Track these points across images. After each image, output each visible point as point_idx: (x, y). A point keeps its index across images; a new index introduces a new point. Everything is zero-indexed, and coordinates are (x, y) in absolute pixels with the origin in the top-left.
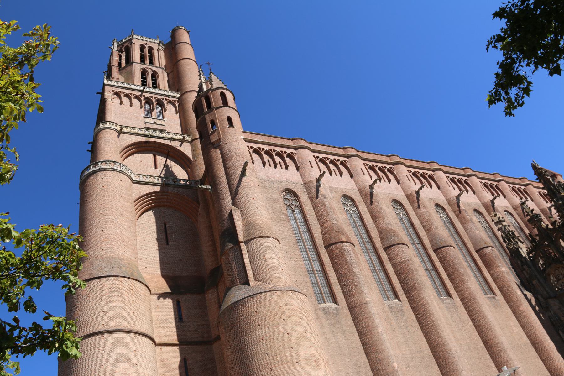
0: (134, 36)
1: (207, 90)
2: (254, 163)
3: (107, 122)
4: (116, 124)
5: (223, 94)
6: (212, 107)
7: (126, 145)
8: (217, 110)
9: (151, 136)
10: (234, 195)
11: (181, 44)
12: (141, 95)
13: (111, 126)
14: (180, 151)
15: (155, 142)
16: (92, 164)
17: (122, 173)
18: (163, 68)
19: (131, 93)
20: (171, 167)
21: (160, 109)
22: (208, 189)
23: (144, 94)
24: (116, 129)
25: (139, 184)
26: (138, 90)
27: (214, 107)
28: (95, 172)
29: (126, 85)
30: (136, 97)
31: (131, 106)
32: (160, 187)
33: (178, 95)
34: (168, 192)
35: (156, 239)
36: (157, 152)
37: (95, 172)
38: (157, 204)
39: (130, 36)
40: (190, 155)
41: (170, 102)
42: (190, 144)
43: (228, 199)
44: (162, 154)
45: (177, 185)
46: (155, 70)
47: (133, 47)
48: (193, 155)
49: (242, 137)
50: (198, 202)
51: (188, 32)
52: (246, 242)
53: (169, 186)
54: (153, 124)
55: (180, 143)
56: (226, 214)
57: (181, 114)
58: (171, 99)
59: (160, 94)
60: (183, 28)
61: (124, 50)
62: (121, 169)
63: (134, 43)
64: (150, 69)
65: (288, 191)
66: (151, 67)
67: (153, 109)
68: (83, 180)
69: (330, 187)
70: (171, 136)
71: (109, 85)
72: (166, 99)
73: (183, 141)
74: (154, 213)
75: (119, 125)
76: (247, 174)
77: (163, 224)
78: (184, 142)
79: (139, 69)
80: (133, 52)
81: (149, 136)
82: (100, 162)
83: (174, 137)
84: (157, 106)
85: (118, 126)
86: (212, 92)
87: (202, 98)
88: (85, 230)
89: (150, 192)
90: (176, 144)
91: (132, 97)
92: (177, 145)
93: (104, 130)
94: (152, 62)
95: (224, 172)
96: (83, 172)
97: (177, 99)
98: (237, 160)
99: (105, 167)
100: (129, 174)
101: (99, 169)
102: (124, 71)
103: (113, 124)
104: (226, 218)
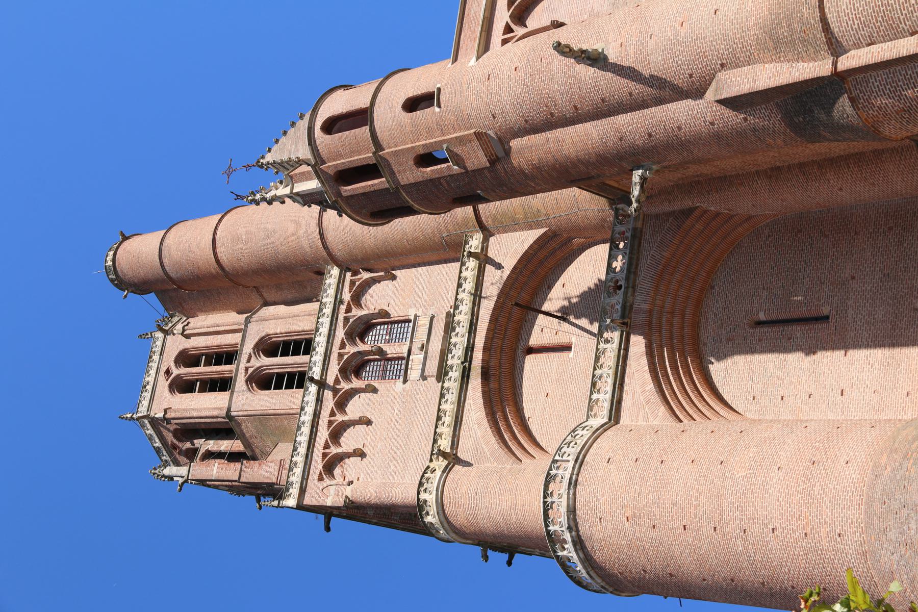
0: (143, 411)
1: (319, 178)
2: (561, 20)
3: (418, 499)
4: (425, 472)
5: (331, 126)
6: (374, 162)
7: (493, 440)
8: (384, 144)
9: (465, 361)
10: (667, 92)
11: (166, 262)
12: (335, 391)
13: (432, 486)
14: (515, 268)
15: (486, 349)
16: (555, 552)
17: (584, 456)
18: (247, 321)
19: (326, 423)
20: (569, 299)
21: (381, 330)
22: (643, 179)
23: (330, 380)
24: (444, 472)
25: (619, 402)
26: (319, 400)
27: (374, 153)
28: (579, 543)
29: (303, 439)
30: (341, 405)
31: (368, 422)
32: (632, 336)
33: (335, 271)
34: (650, 312)
35: (807, 354)
36: (518, 341)
37: (579, 543)
38: (687, 348)
39: (143, 426)
40: (529, 237)
41: (357, 299)
42: (492, 235)
44: (524, 326)
45: (627, 279)
46: (252, 346)
47: (178, 415)
48: (531, 228)
49: (473, 62)
50: (687, 213)
51: (125, 238)
52: (836, 48)
53: (631, 306)
54: (426, 353)
55: (489, 268)
56: (733, 118)
57: (397, 263)
58: (347, 296)
59: (330, 330)
60: (111, 253)
61: (188, 445)
62: (572, 458)
63: (165, 411)
64: (249, 361)
66: (244, 358)
67: (380, 352)
68: (603, 584)
70: (466, 297)
71: (303, 491)
72: (348, 310)
73: (482, 257)
74: (719, 358)
75: (431, 460)
76: (599, 47)
77: (758, 330)
78: (486, 255)
79: (249, 394)
80: (195, 414)
81: (464, 367)
82: (547, 526)
83: (469, 286)
84: (370, 338)
85: (432, 465)
86: (324, 162)
87: (344, 194)
88: (771, 589)
89: (647, 368)
90: (494, 281)
91: (340, 418)
92: (497, 277)
93: (446, 509)
94: (228, 356)
95: (588, 125)
96: (579, 582)
97: (349, 274)
98: (551, 81)
99: (563, 509)
100: (587, 434)
101: (570, 528)
102: (256, 442)
103: (428, 479)
104: (745, 119)
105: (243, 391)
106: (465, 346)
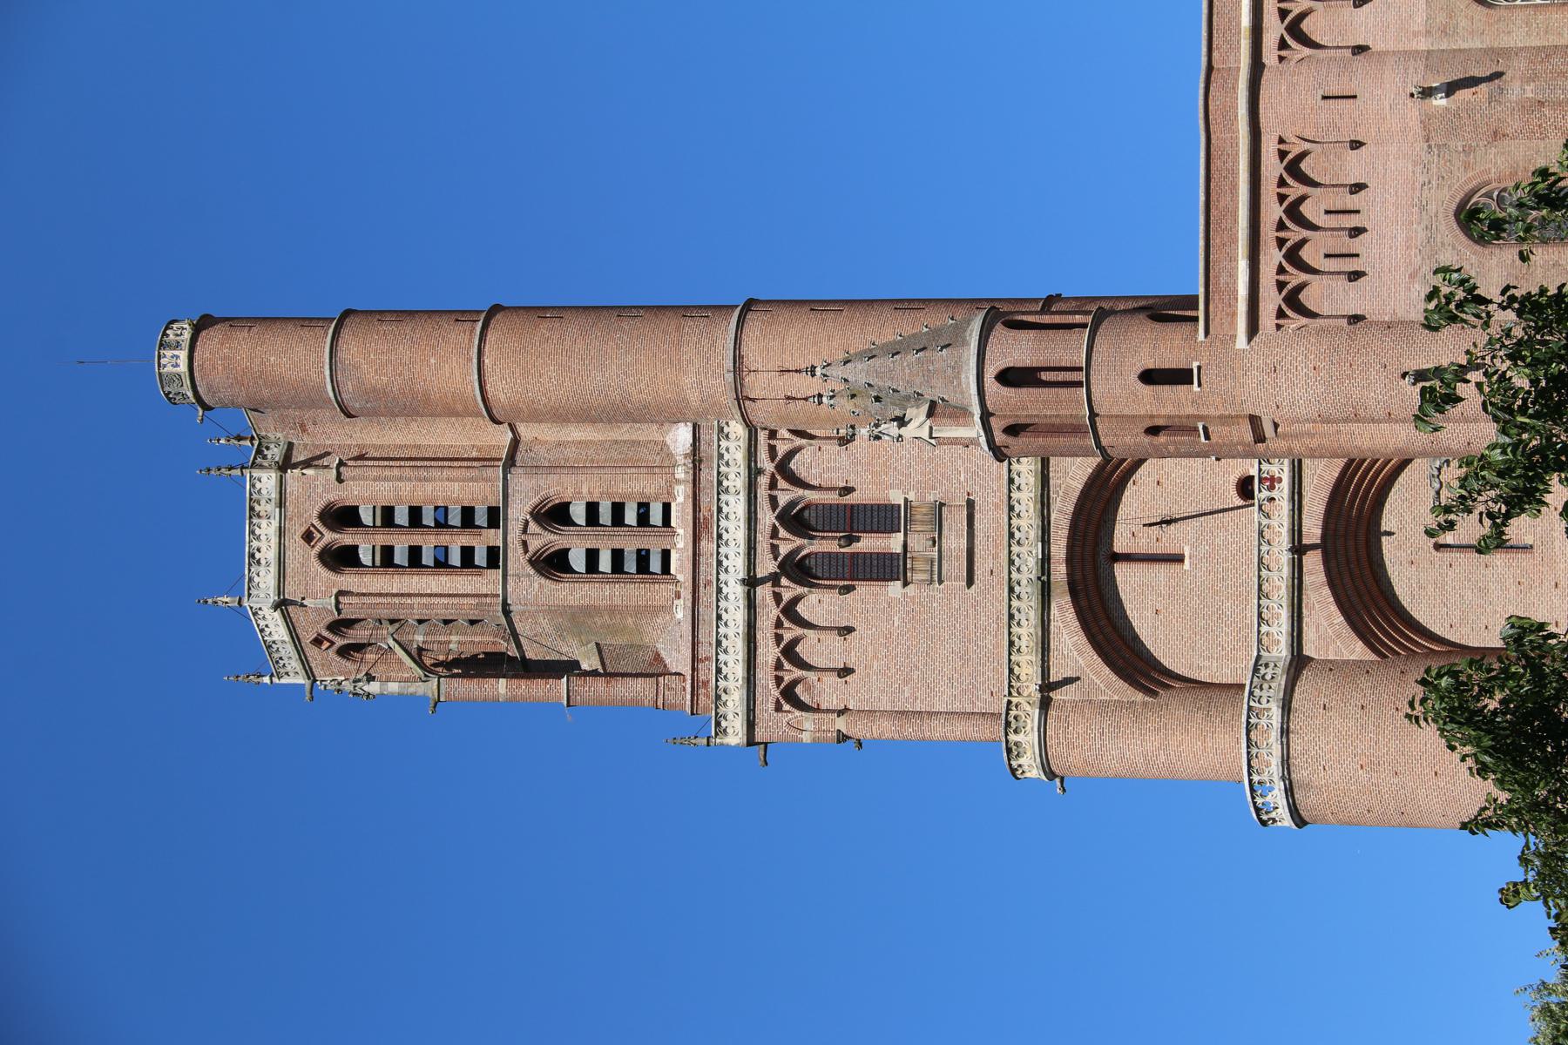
5: (1009, 377)
15: (1069, 560)
36: (1096, 544)
69: (1428, 32)
71: (751, 725)
72: (773, 485)
81: (1043, 582)
101: (1283, 778)
105: (529, 575)
106: (1040, 557)
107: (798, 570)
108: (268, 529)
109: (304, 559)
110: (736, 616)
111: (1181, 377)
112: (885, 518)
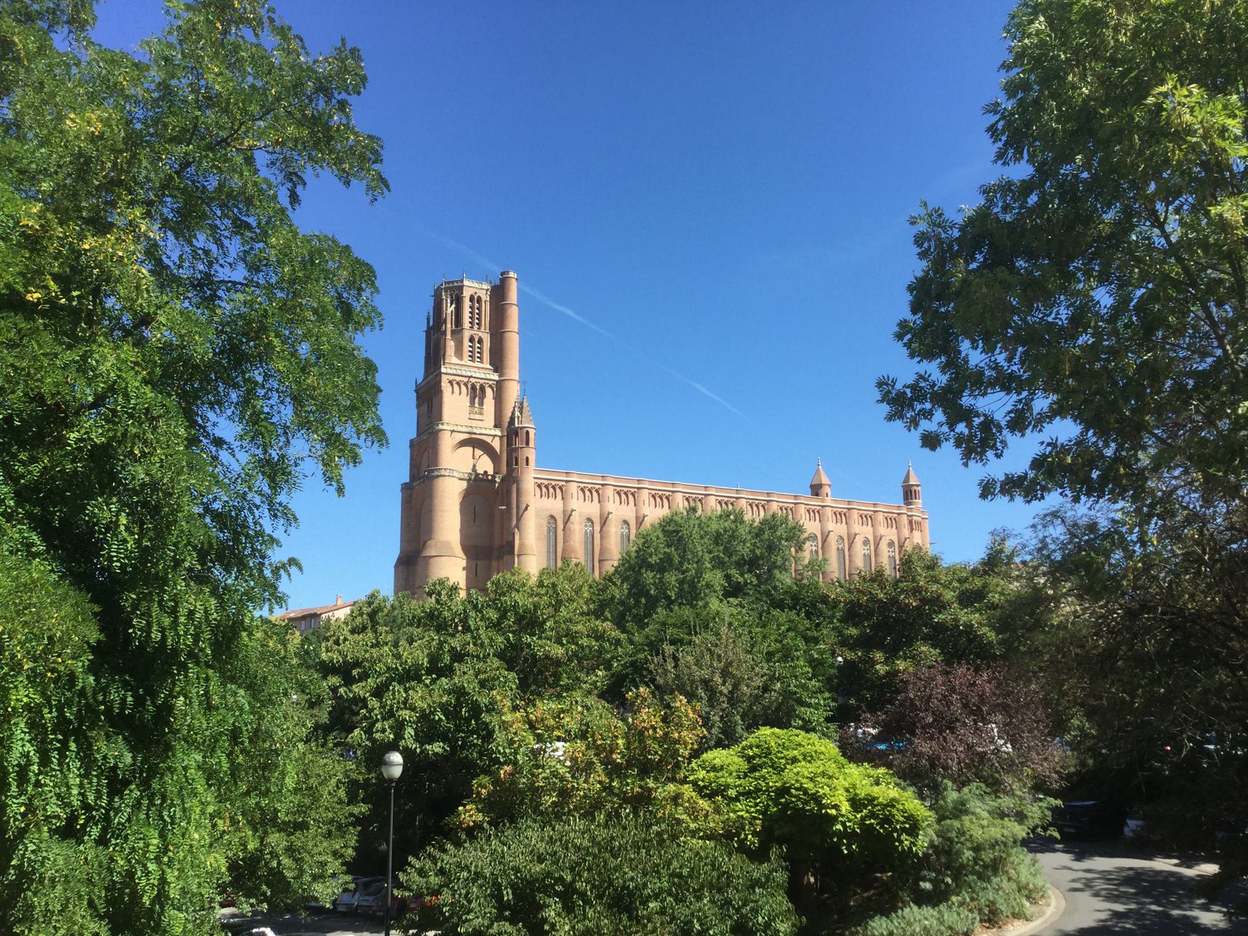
5: (527, 432)
23: (471, 379)
40: (498, 450)
43: (514, 522)
58: (491, 382)
65: (552, 517)
90: (489, 440)
107: (473, 387)
108: (476, 285)
109: (471, 291)
110: (464, 373)
111: (527, 464)
112: (481, 404)
